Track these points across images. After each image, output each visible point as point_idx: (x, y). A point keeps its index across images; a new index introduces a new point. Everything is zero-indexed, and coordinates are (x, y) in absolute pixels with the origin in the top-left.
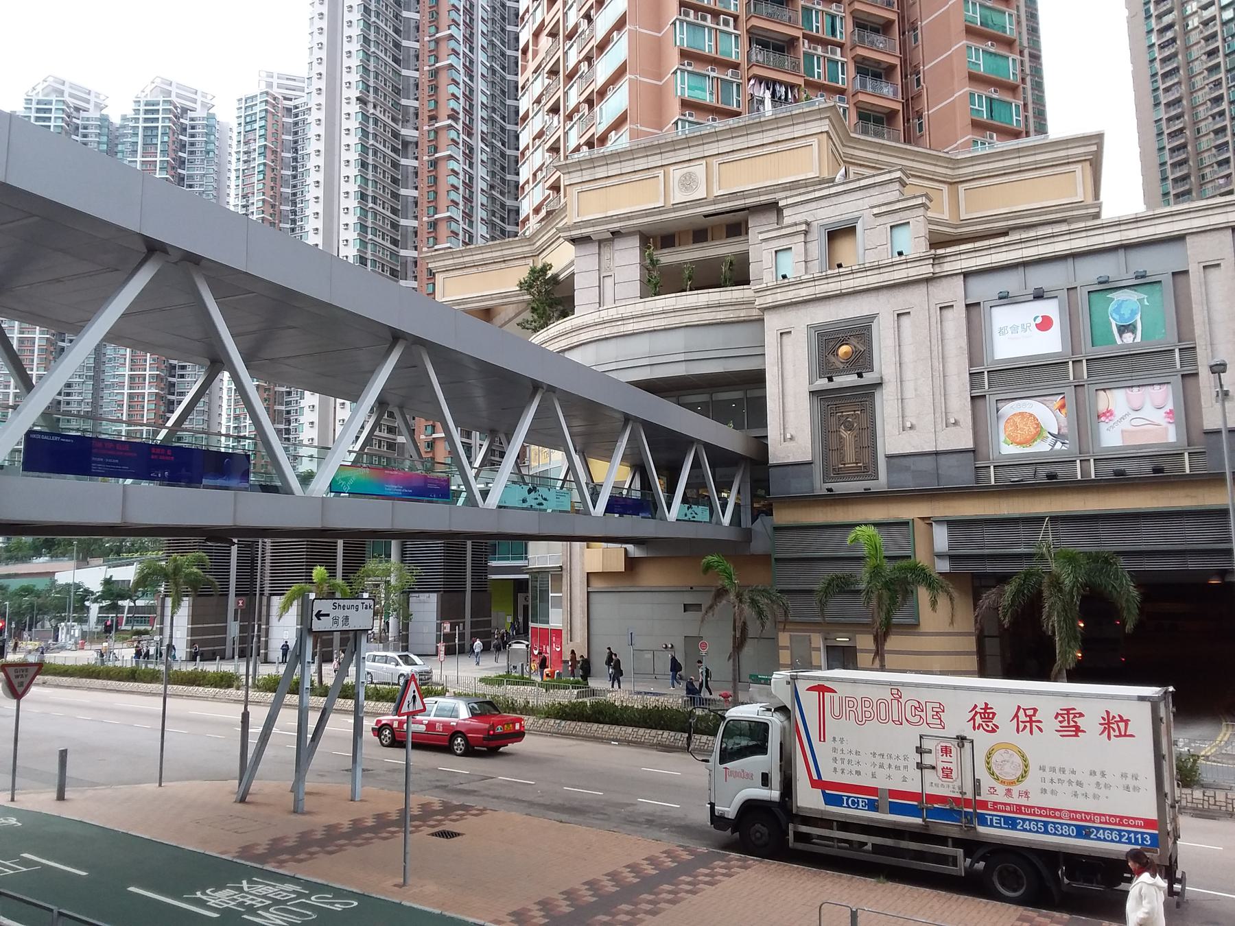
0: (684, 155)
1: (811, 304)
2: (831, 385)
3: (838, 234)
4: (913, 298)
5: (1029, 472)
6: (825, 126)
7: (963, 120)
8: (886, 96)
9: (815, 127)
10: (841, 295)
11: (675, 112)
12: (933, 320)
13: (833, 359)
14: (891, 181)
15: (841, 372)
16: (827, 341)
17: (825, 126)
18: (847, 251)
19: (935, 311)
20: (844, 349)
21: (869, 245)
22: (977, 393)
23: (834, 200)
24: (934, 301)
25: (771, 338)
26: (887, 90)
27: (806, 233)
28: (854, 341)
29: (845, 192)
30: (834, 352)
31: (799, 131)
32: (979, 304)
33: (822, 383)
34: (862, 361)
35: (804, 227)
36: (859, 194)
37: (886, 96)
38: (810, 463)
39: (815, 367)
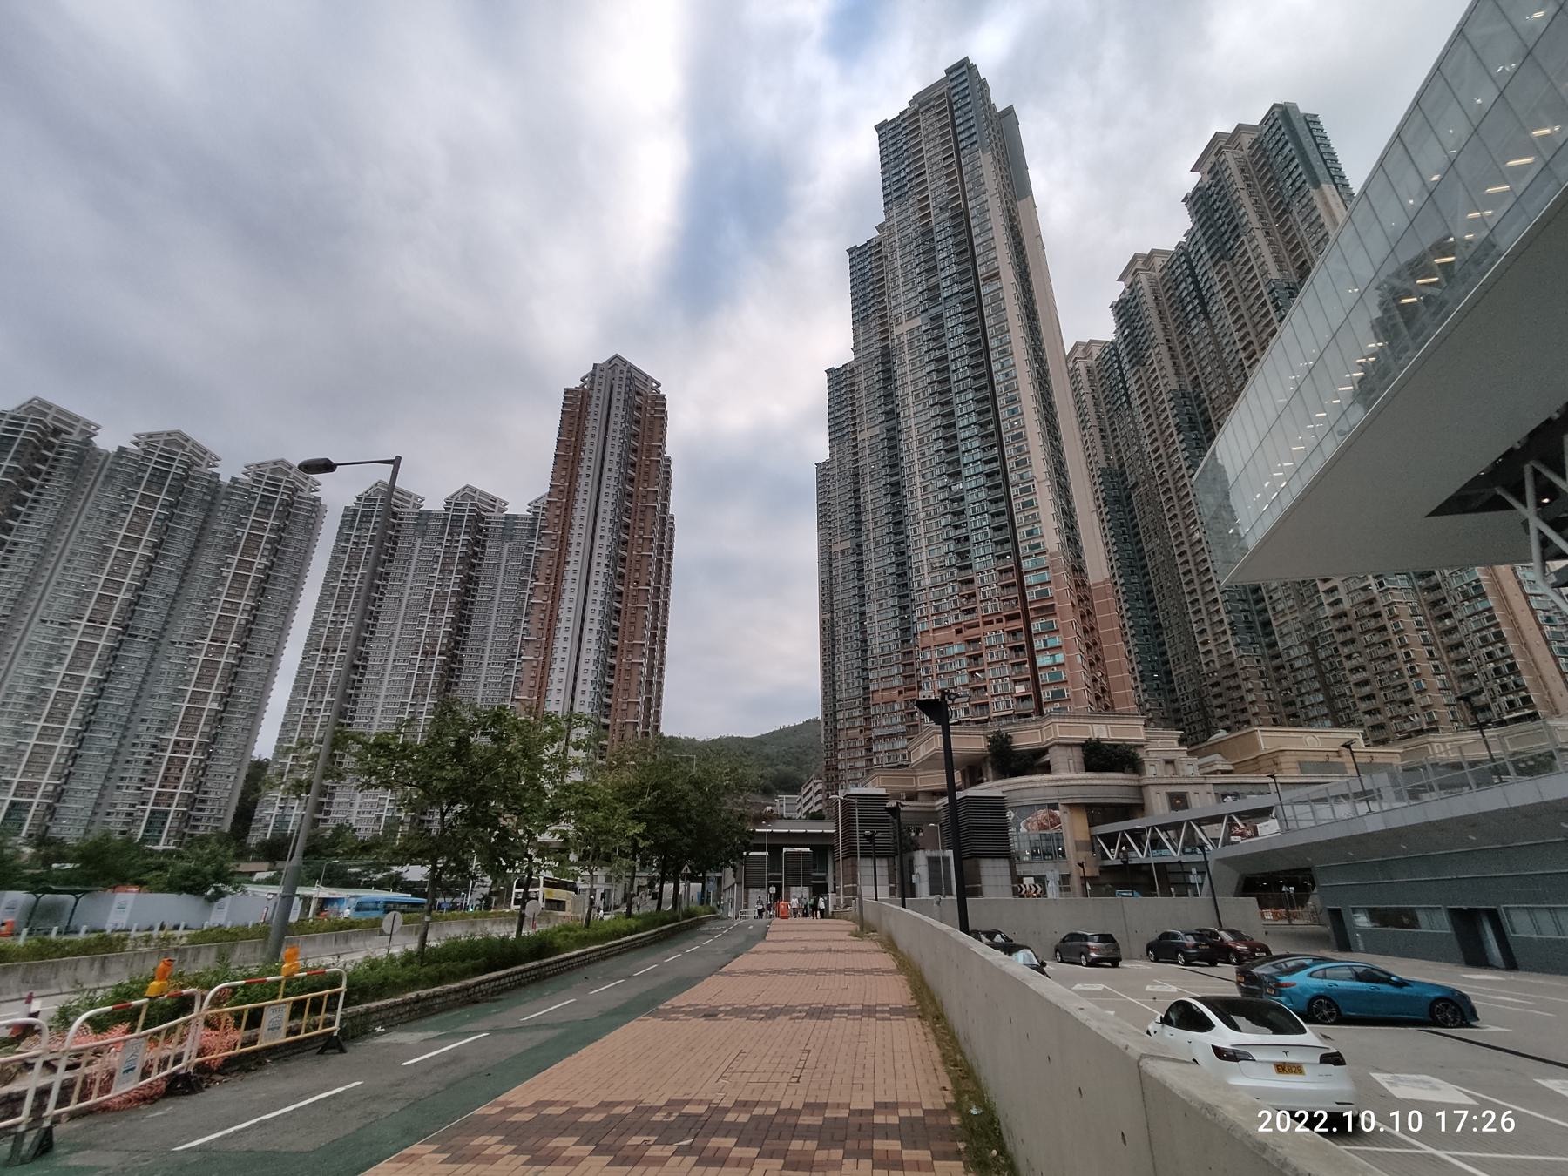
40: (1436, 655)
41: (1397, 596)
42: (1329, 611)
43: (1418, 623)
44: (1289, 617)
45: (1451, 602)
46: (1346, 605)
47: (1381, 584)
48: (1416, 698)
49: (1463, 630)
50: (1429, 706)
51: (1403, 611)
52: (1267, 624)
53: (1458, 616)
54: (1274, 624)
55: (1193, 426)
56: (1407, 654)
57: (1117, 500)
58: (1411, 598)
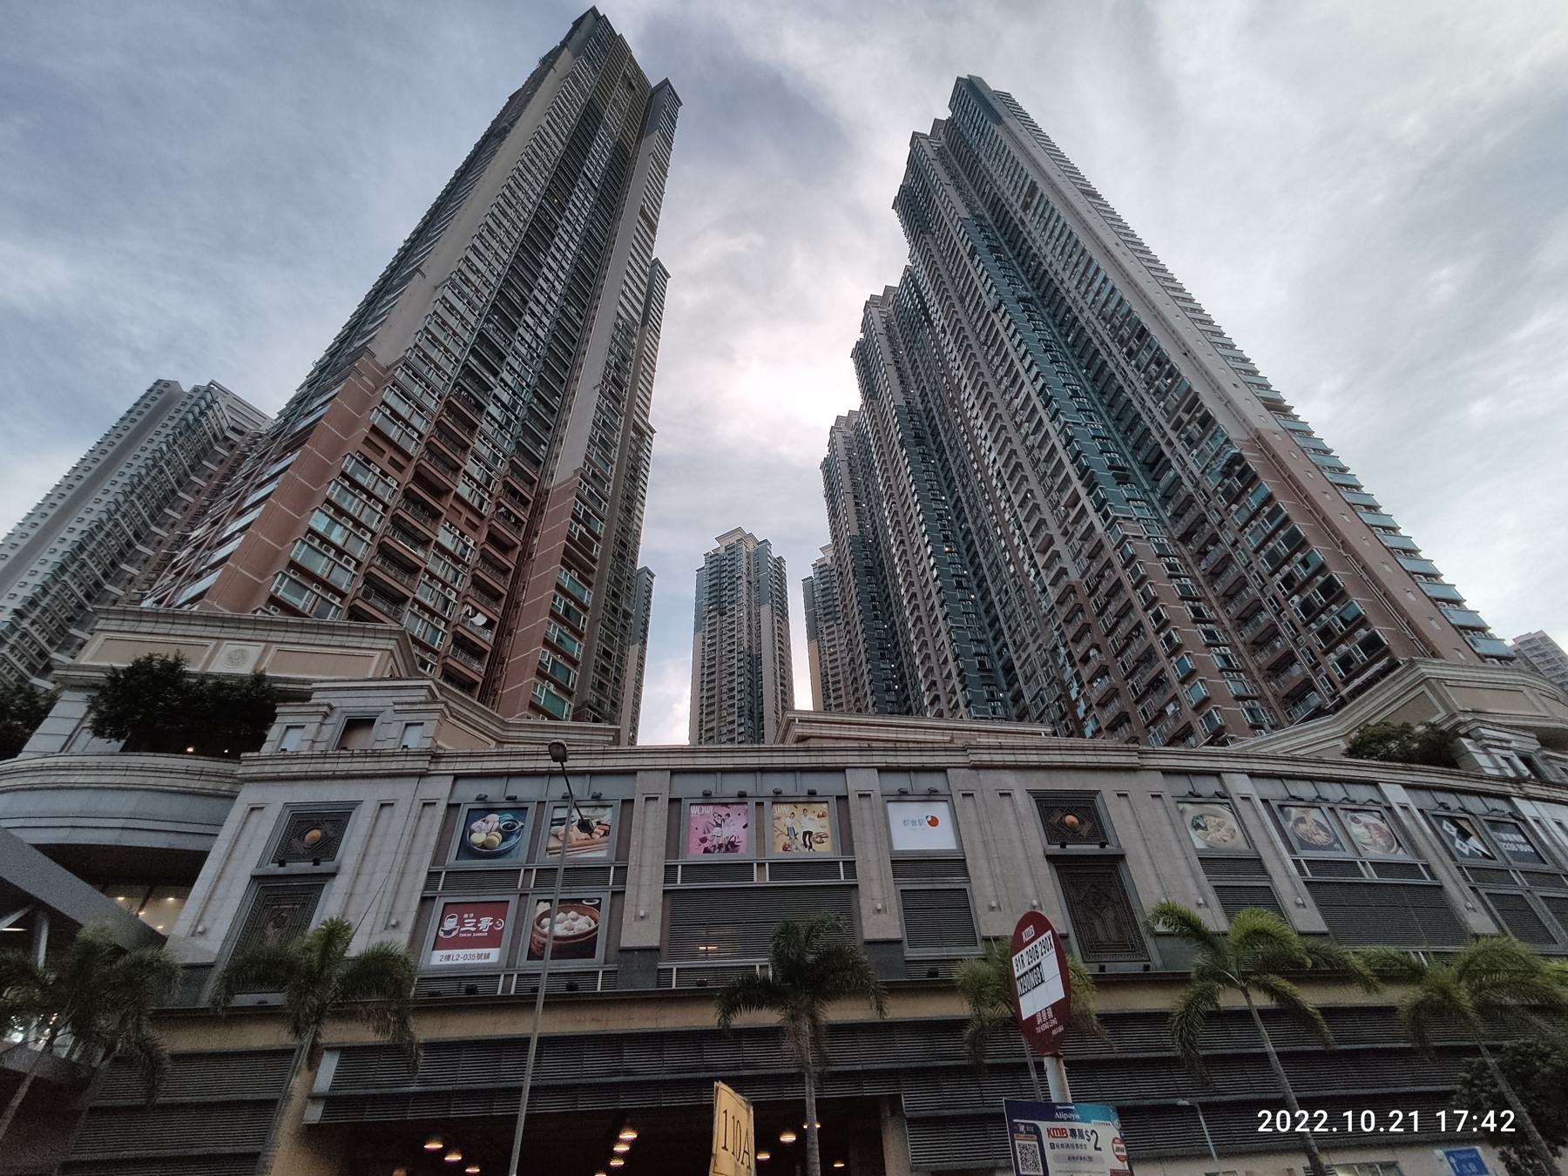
0: (248, 634)
1: (301, 783)
2: (281, 871)
3: (358, 723)
4: (403, 791)
5: (453, 985)
6: (392, 645)
7: (524, 700)
8: (476, 670)
9: (381, 644)
10: (334, 777)
11: (261, 601)
12: (413, 814)
13: (295, 841)
14: (421, 687)
15: (299, 858)
16: (300, 820)
17: (392, 645)
18: (360, 741)
19: (417, 805)
20: (316, 833)
21: (385, 735)
22: (429, 894)
23: (366, 693)
24: (420, 796)
25: (238, 810)
26: (476, 666)
27: (326, 715)
28: (328, 826)
29: (378, 688)
30: (301, 836)
31: (366, 643)
32: (458, 805)
33: (274, 869)
34: (327, 848)
35: (325, 709)
36: (390, 693)
37: (476, 670)
38: (210, 966)
39: (273, 849)
40: (1221, 638)
41: (1130, 529)
42: (1053, 594)
43: (1171, 567)
44: (1032, 648)
45: (1213, 519)
46: (1074, 576)
47: (1106, 516)
48: (1182, 691)
49: (1240, 559)
50: (1206, 701)
51: (1146, 552)
52: (1009, 668)
53: (1227, 537)
54: (1017, 664)
55: (920, 439)
56: (1158, 617)
57: (869, 571)
58: (1156, 530)
